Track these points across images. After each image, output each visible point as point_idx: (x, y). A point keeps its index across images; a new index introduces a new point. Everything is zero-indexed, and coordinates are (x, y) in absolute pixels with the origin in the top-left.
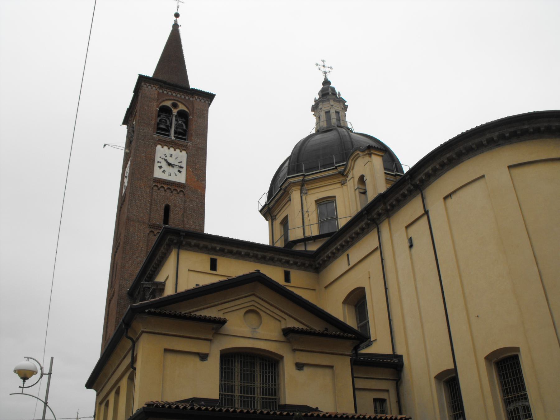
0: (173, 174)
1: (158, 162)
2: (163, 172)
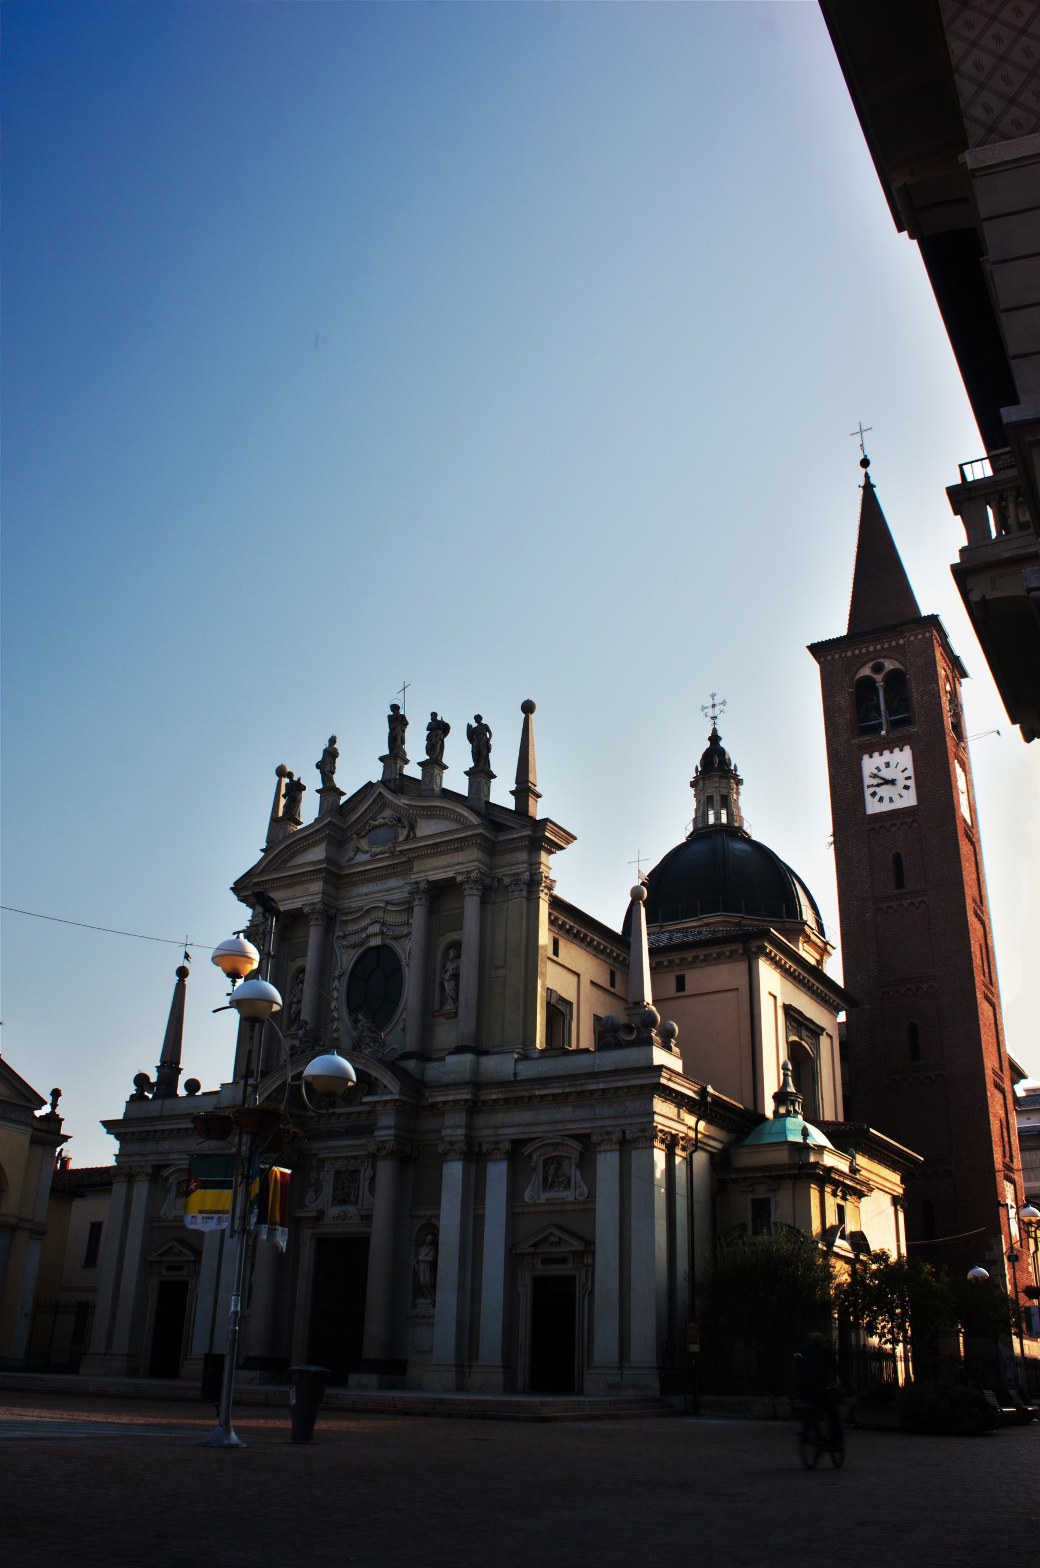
0: (896, 798)
1: (869, 787)
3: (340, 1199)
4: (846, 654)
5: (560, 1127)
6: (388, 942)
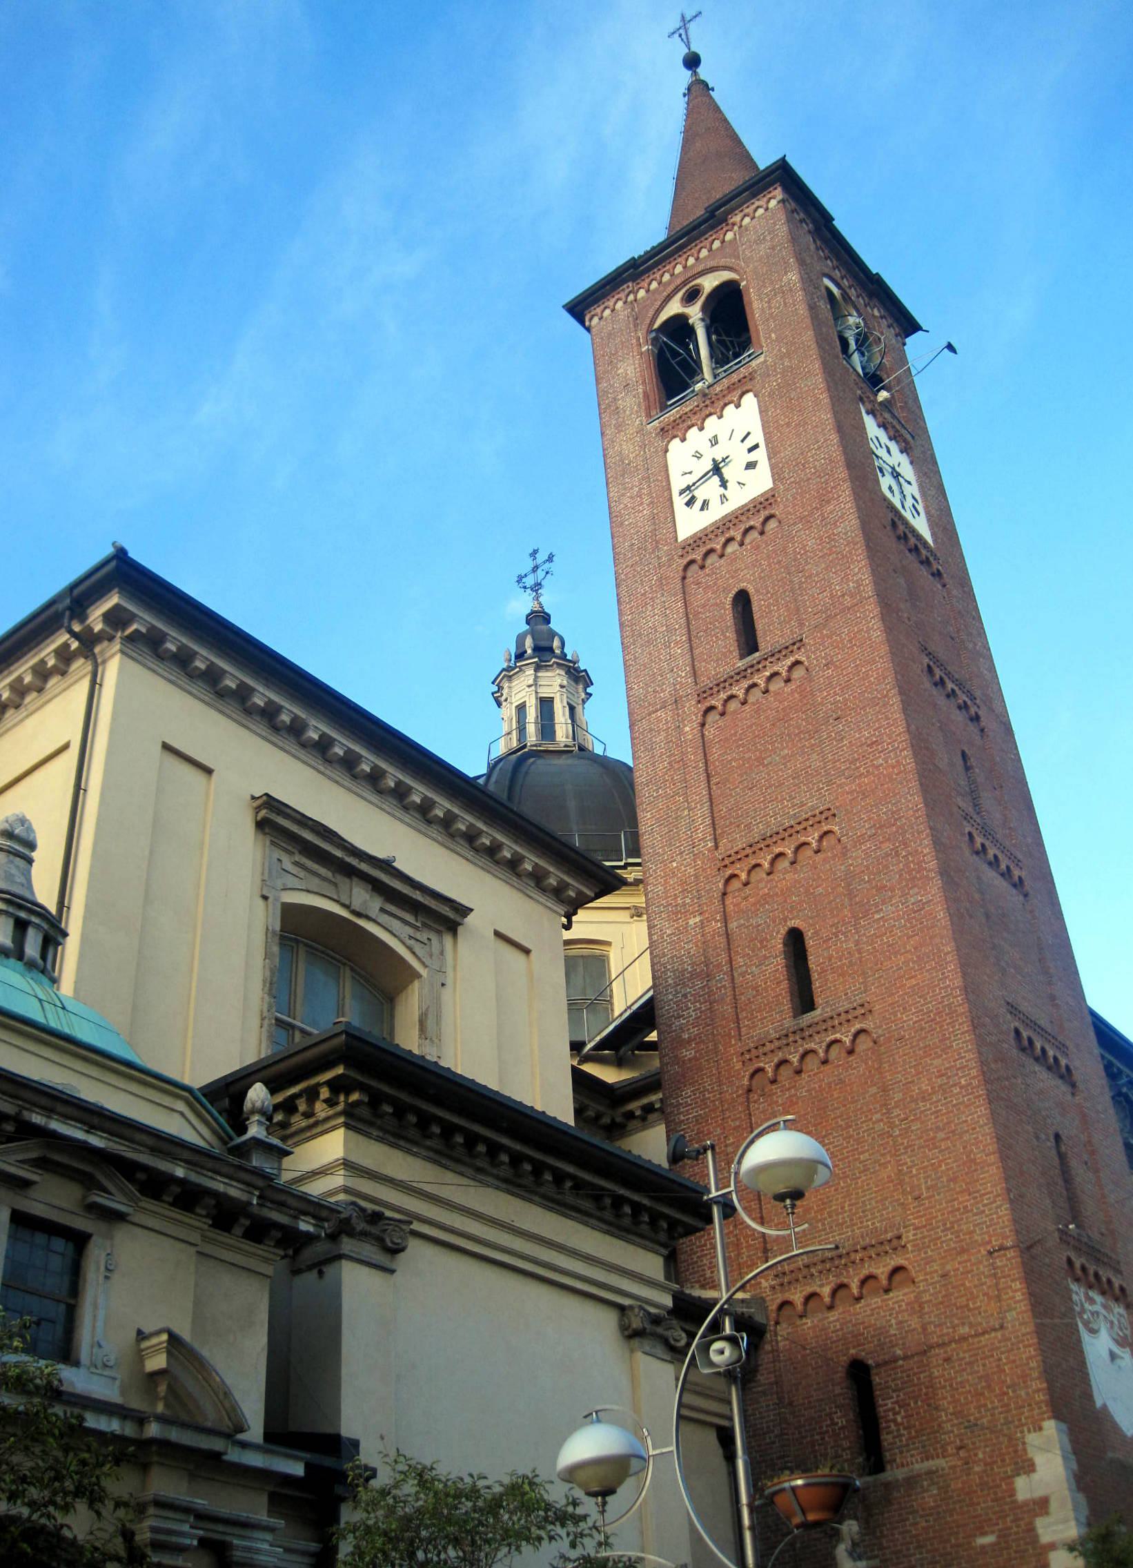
2: (702, 509)
4: (636, 297)
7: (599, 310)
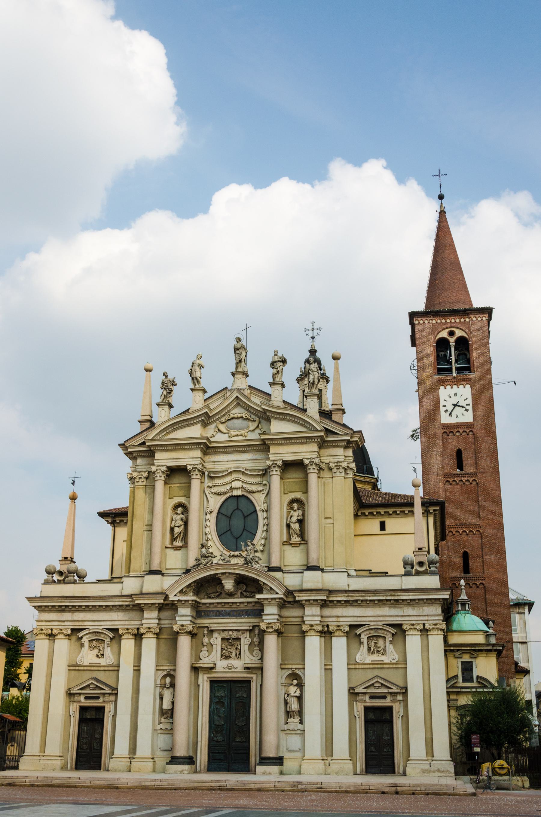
0: (460, 415)
1: (443, 406)
3: (225, 657)
5: (381, 619)
6: (245, 493)
7: (419, 319)
